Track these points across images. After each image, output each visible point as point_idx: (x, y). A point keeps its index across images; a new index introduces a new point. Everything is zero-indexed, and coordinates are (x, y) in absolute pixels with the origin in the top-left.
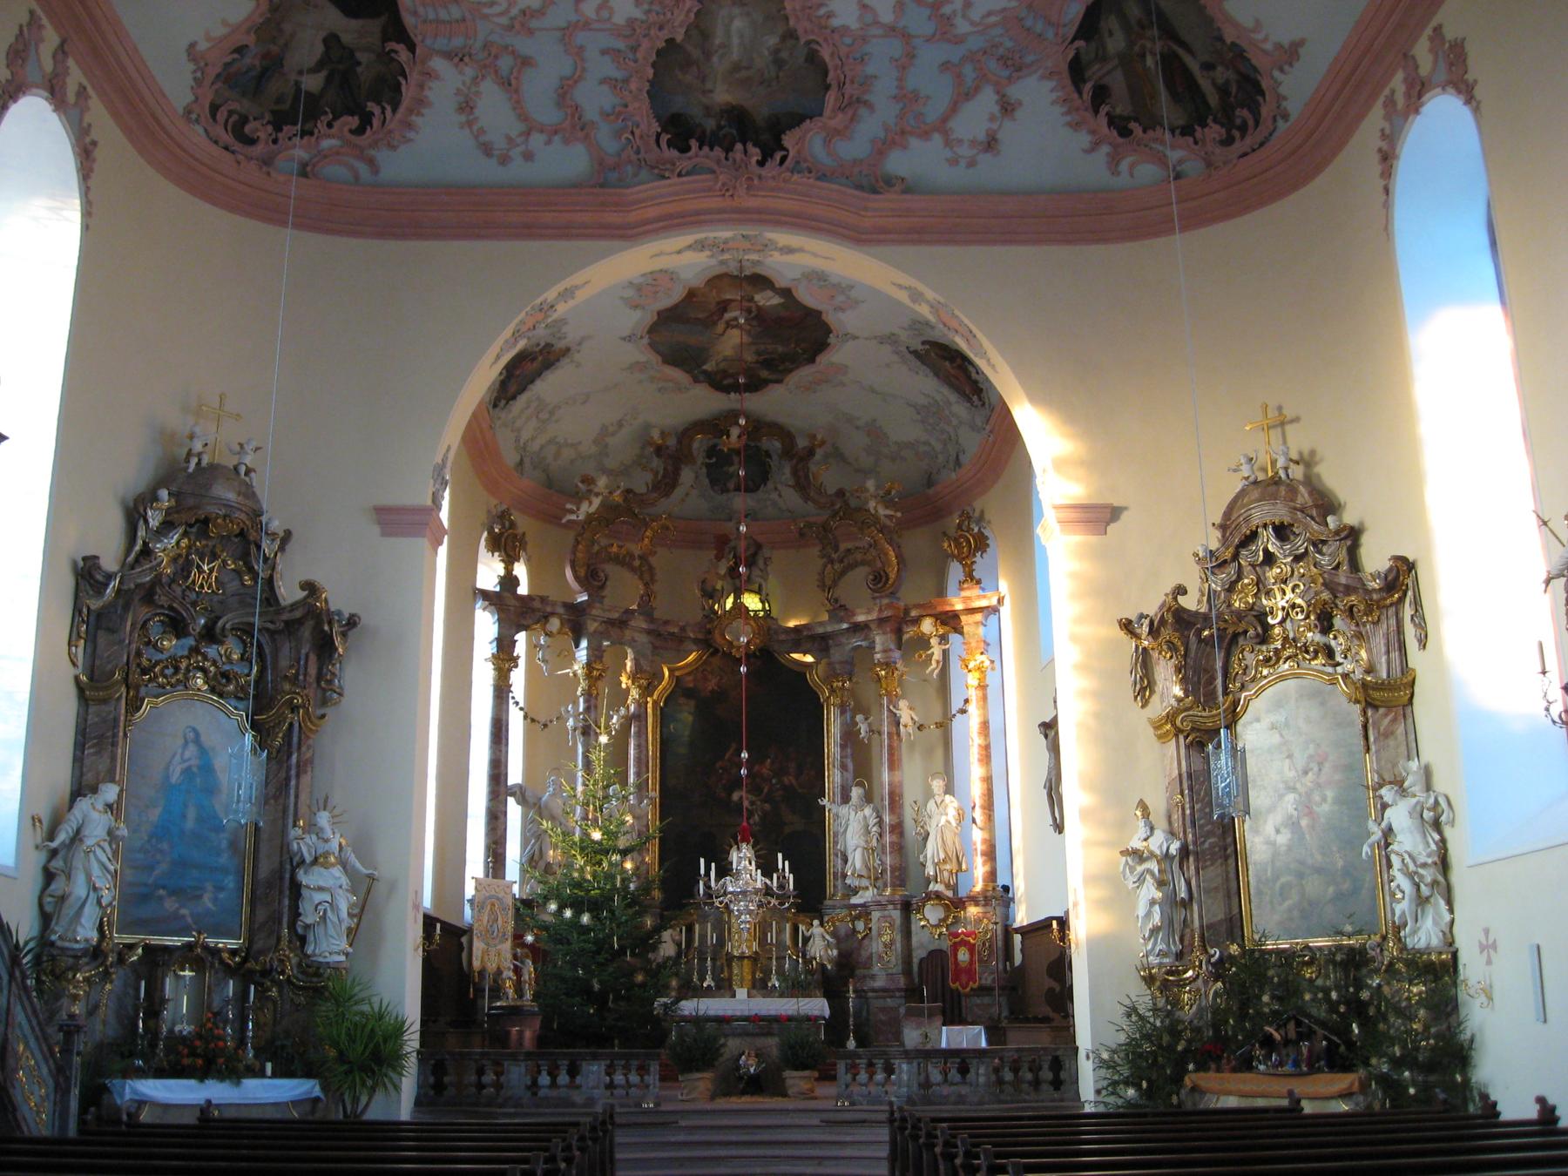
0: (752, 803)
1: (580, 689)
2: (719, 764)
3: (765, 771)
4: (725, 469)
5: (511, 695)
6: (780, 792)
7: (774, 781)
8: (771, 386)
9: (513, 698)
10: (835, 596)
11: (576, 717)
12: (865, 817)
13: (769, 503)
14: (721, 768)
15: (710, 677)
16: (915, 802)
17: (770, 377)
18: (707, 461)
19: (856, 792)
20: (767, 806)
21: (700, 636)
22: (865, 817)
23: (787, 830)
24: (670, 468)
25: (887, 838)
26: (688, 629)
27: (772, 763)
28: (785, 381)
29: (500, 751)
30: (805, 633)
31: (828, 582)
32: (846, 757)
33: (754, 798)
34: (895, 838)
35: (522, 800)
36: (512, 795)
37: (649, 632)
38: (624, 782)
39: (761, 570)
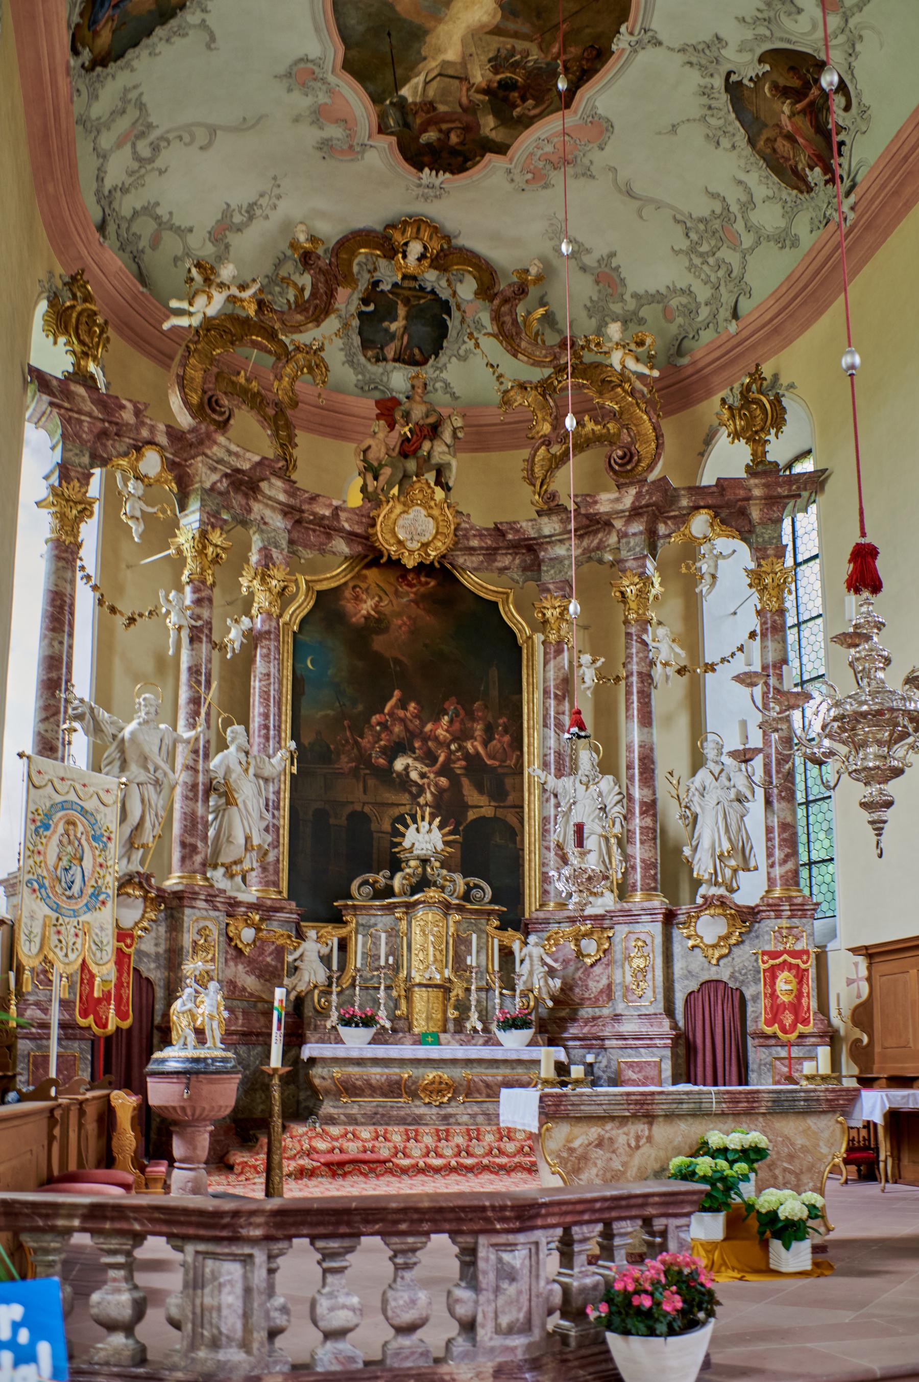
0: (423, 775)
1: (186, 573)
2: (375, 719)
3: (441, 733)
4: (386, 324)
5: (79, 563)
6: (463, 763)
7: (453, 747)
8: (489, 156)
9: (83, 568)
10: (553, 487)
11: (182, 610)
12: (600, 794)
13: (439, 385)
14: (379, 724)
15: (364, 597)
16: (671, 774)
17: (493, 135)
18: (364, 309)
19: (586, 758)
20: (443, 781)
21: (359, 530)
22: (600, 794)
23: (472, 815)
24: (322, 288)
25: (637, 822)
26: (343, 515)
27: (451, 722)
28: (510, 153)
29: (61, 643)
30: (510, 537)
31: (539, 472)
32: (563, 713)
33: (425, 769)
34: (648, 821)
35: (96, 729)
36: (79, 717)
37: (288, 511)
38: (245, 721)
39: (448, 446)
